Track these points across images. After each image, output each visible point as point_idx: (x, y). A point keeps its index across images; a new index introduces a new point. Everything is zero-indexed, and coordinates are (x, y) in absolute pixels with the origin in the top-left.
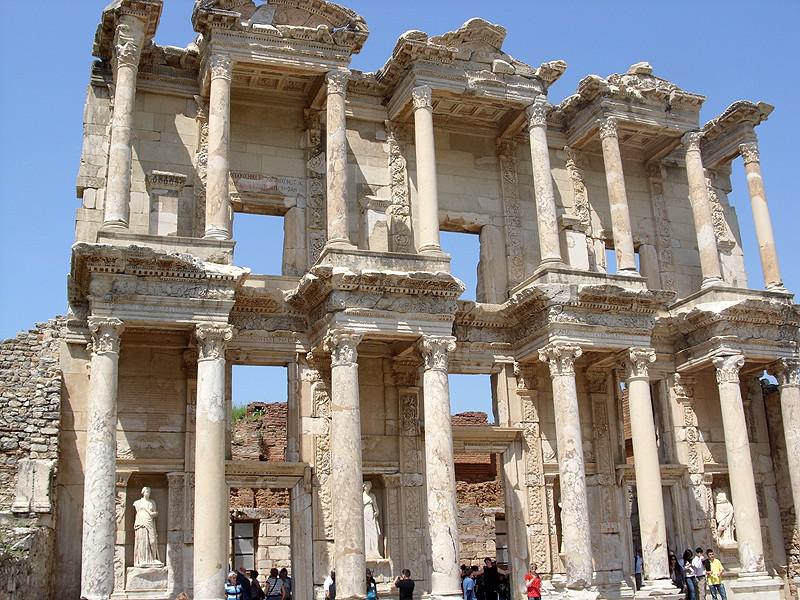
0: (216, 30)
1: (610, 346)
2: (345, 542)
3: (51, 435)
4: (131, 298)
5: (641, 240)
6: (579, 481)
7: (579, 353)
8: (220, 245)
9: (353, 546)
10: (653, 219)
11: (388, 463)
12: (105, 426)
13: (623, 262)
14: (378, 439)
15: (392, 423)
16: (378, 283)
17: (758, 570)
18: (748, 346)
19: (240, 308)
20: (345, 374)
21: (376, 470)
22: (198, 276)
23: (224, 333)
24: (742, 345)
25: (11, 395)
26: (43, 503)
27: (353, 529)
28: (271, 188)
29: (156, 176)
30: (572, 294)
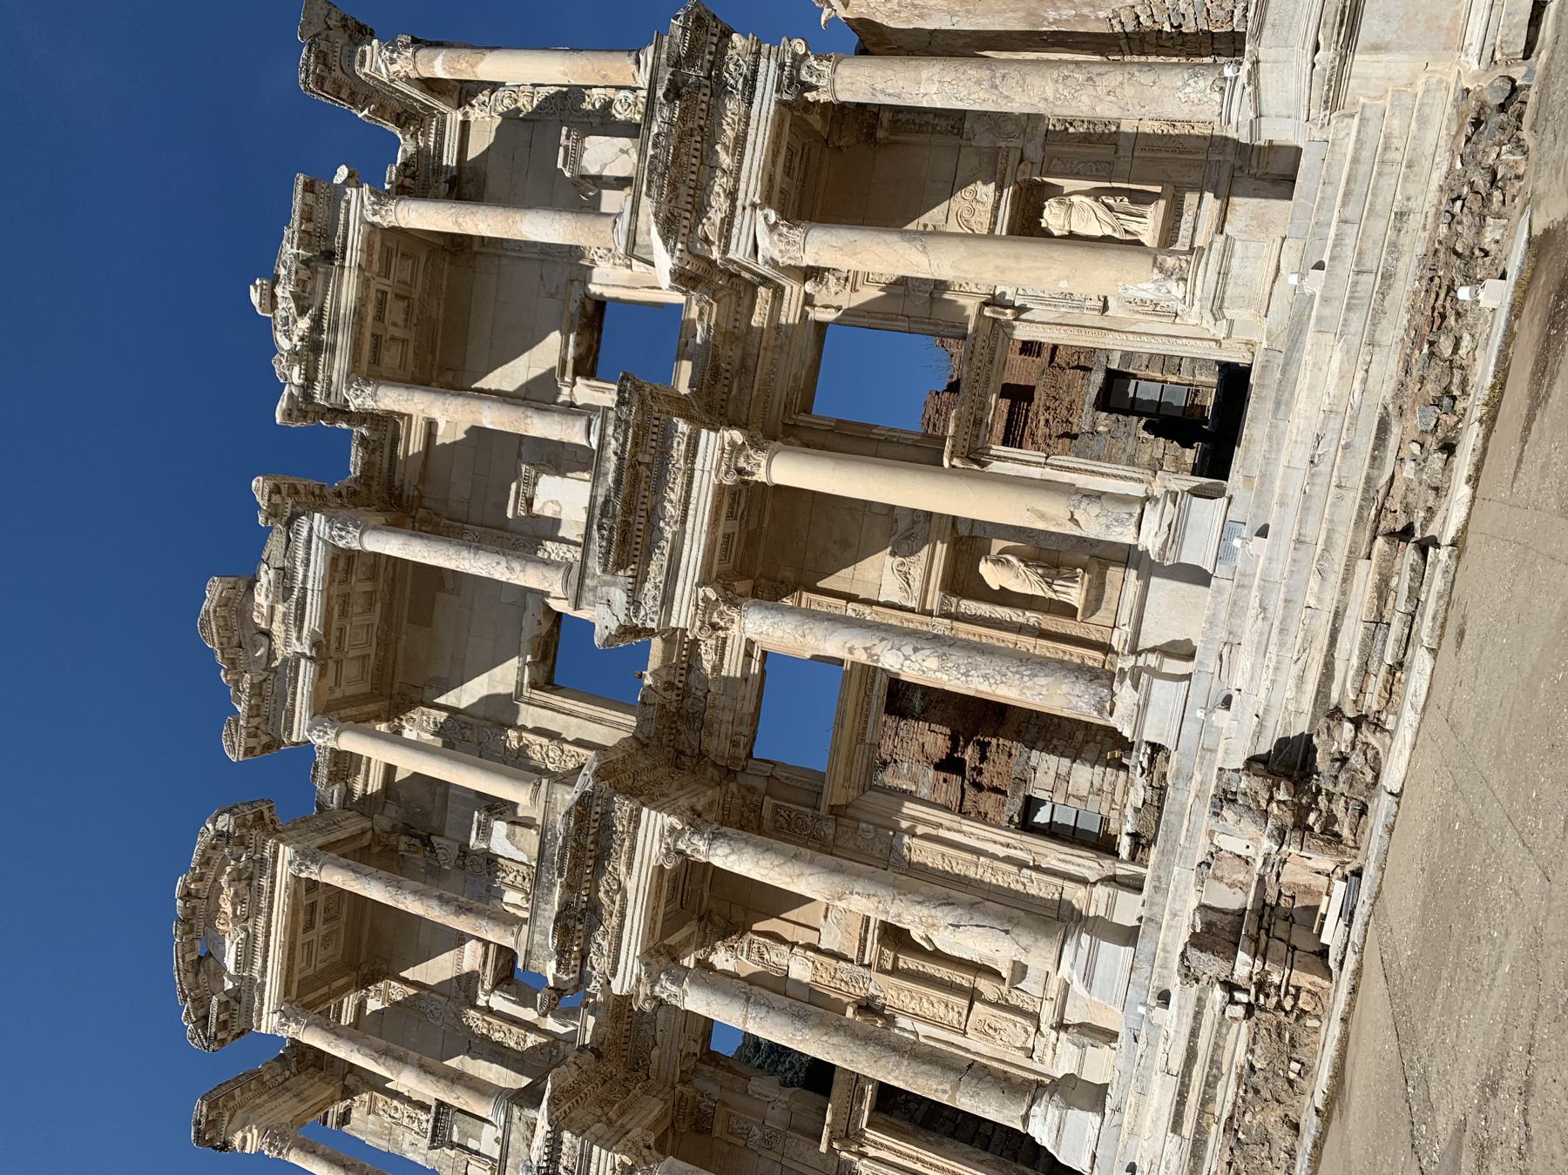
1: (705, 527)
5: (577, 294)
6: (919, 656)
9: (945, 1092)
16: (571, 923)
18: (742, 186)
23: (622, 1164)
24: (739, 203)
27: (921, 1081)
30: (614, 584)
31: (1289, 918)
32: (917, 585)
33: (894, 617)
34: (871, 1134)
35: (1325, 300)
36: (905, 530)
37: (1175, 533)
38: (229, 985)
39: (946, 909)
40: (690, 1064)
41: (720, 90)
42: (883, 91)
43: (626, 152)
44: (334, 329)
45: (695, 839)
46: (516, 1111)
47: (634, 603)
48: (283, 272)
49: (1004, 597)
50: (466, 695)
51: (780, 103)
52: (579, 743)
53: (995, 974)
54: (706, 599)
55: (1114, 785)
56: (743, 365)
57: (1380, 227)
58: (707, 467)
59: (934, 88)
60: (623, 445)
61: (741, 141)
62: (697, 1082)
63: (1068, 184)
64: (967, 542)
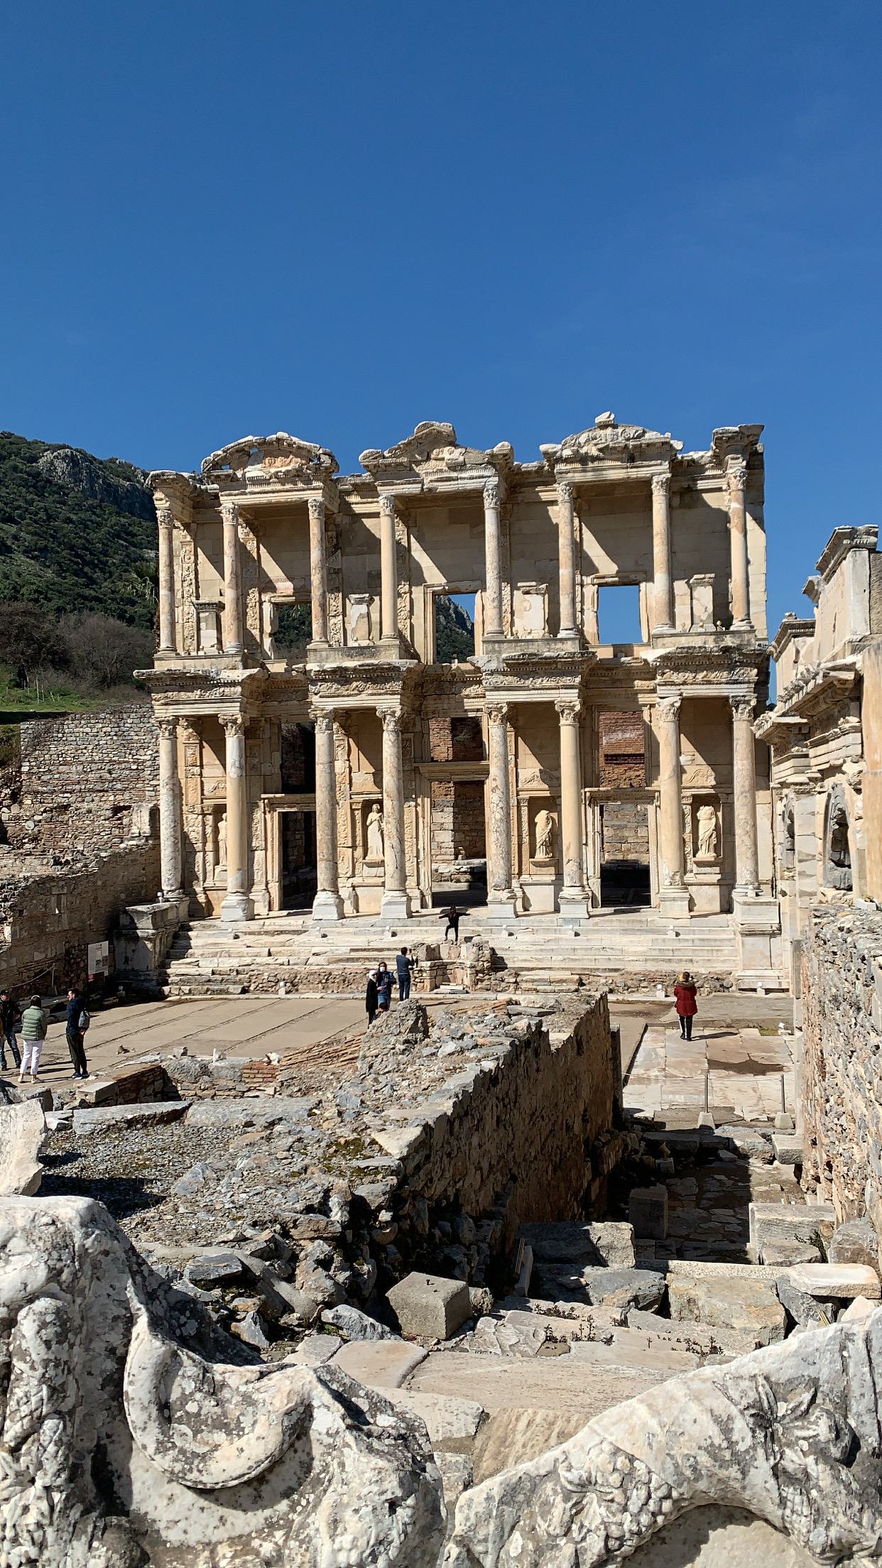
4: (177, 703)
7: (504, 710)
8: (233, 656)
26: (146, 829)
31: (444, 974)
32: (529, 786)
33: (512, 778)
34: (276, 815)
35: (664, 940)
36: (551, 774)
37: (572, 901)
38: (239, 474)
40: (275, 721)
41: (731, 668)
44: (594, 470)
46: (239, 659)
47: (492, 673)
48: (620, 430)
49: (532, 825)
50: (418, 554)
52: (412, 626)
53: (365, 854)
55: (445, 854)
56: (615, 681)
57: (689, 955)
61: (709, 682)
62: (268, 726)
63: (720, 814)
64: (553, 803)
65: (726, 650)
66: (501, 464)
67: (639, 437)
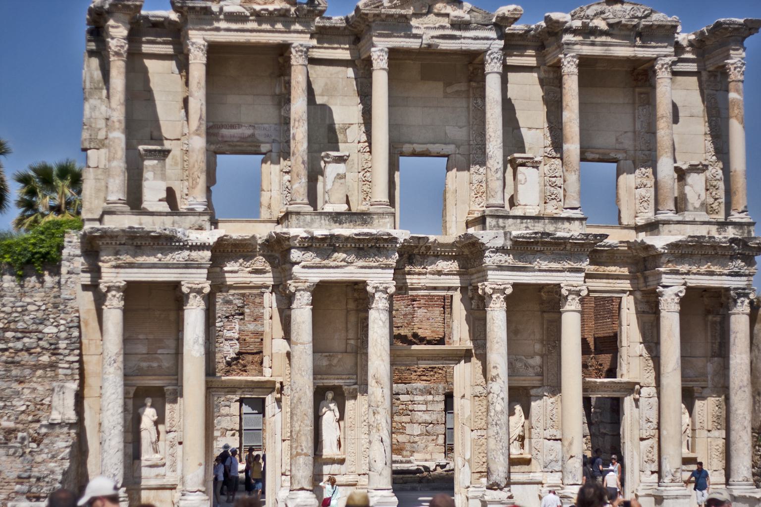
0: (191, 17)
2: (296, 448)
3: (73, 362)
4: (131, 266)
5: (620, 156)
6: (500, 401)
7: (509, 291)
8: (200, 214)
9: (302, 450)
10: (634, 132)
11: (348, 376)
12: (115, 362)
13: (567, 201)
14: (340, 356)
15: (352, 342)
16: (328, 241)
17: (673, 481)
19: (222, 250)
20: (302, 313)
21: (336, 382)
22: (181, 244)
25: (28, 300)
26: (72, 417)
28: (249, 136)
29: (146, 150)
30: (506, 239)
38: (215, 8)
39: (387, 434)
42: (736, 337)
43: (699, 198)
45: (385, 301)
46: (206, 218)
47: (497, 250)
51: (728, 290)
54: (505, 289)
58: (568, 279)
59: (738, 361)
60: (576, 239)
61: (712, 273)
65: (733, 240)
66: (500, 25)
67: (646, 17)
